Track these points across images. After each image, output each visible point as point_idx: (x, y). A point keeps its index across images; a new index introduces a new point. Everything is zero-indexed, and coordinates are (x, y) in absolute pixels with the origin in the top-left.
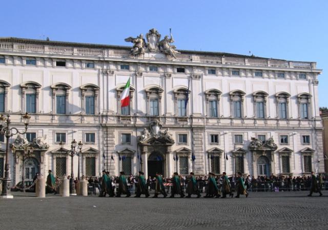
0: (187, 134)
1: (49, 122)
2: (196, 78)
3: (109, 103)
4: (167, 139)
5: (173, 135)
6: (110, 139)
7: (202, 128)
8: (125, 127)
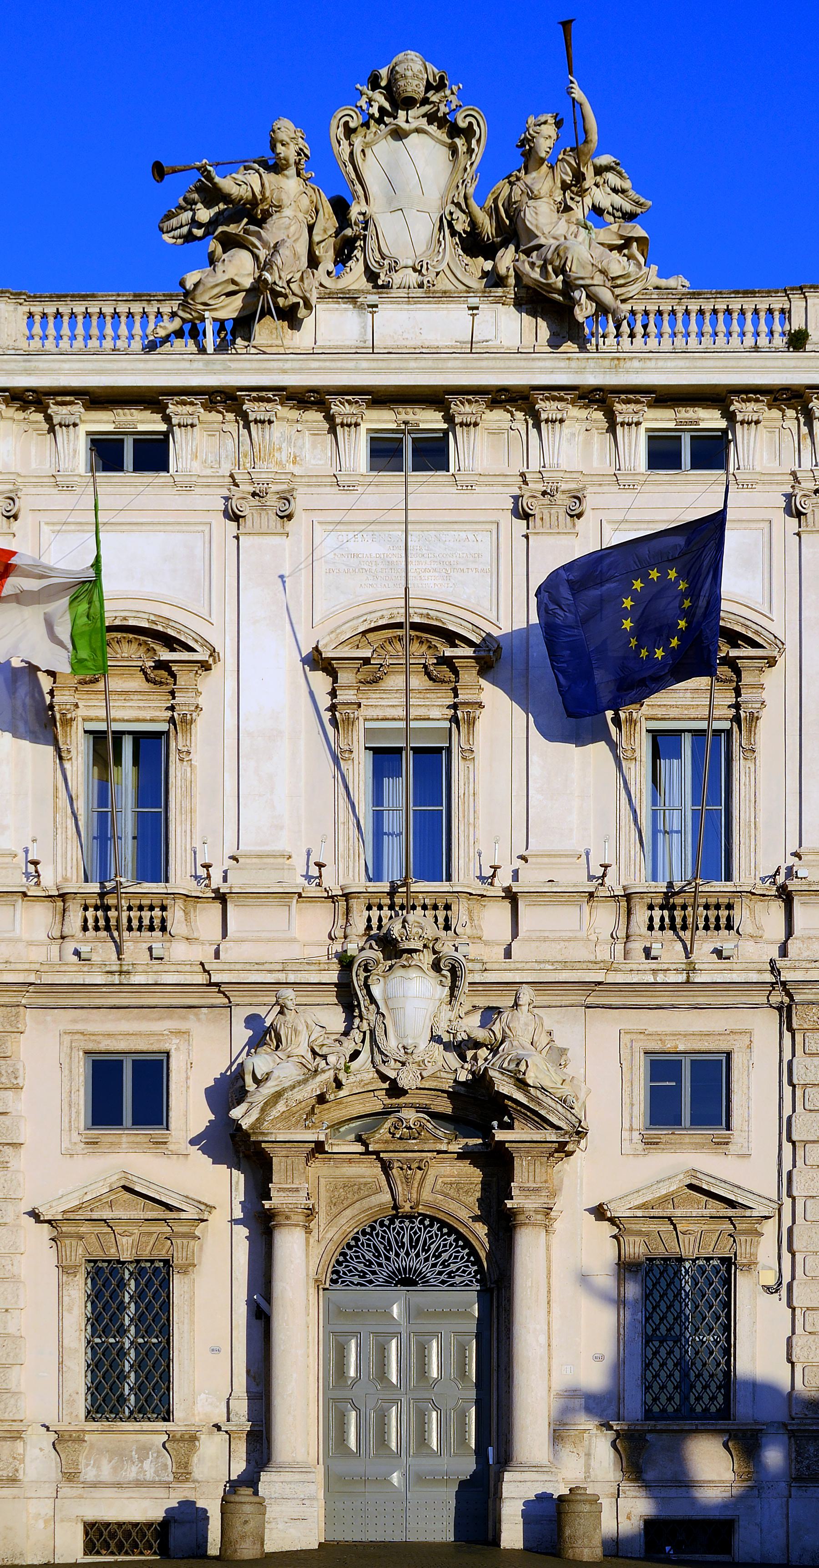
5: (591, 1069)
8: (121, 993)
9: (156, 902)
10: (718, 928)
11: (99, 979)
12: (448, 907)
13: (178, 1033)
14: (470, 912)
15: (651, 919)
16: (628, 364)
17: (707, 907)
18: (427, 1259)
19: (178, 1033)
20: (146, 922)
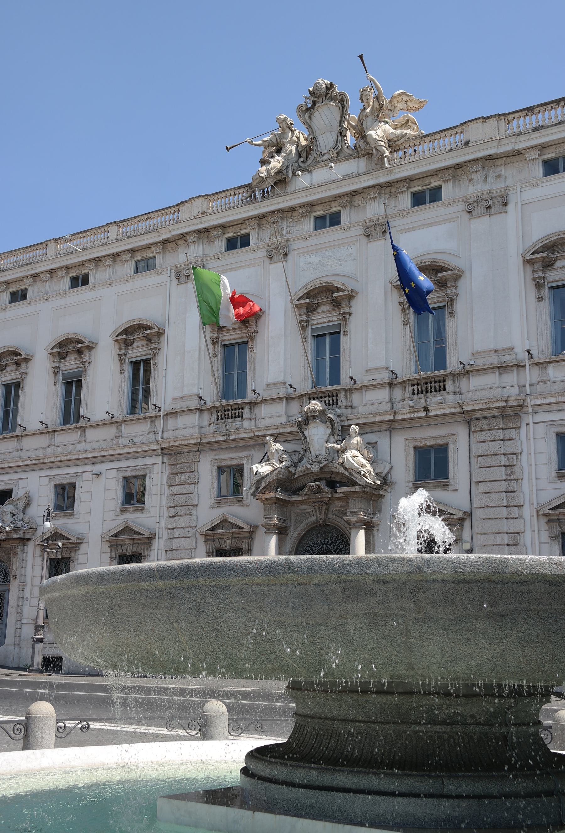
0: (450, 441)
1: (40, 453)
2: (489, 208)
3: (186, 369)
4: (341, 470)
6: (184, 489)
7: (509, 414)
9: (240, 406)
10: (440, 390)
11: (221, 439)
12: (337, 396)
13: (247, 456)
14: (346, 396)
15: (414, 390)
16: (394, 171)
17: (435, 382)
18: (331, 544)
19: (247, 456)
20: (237, 414)
